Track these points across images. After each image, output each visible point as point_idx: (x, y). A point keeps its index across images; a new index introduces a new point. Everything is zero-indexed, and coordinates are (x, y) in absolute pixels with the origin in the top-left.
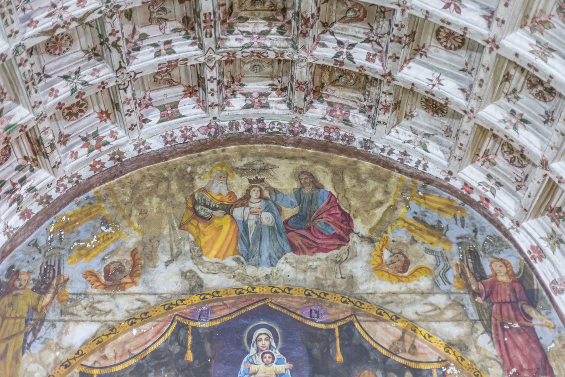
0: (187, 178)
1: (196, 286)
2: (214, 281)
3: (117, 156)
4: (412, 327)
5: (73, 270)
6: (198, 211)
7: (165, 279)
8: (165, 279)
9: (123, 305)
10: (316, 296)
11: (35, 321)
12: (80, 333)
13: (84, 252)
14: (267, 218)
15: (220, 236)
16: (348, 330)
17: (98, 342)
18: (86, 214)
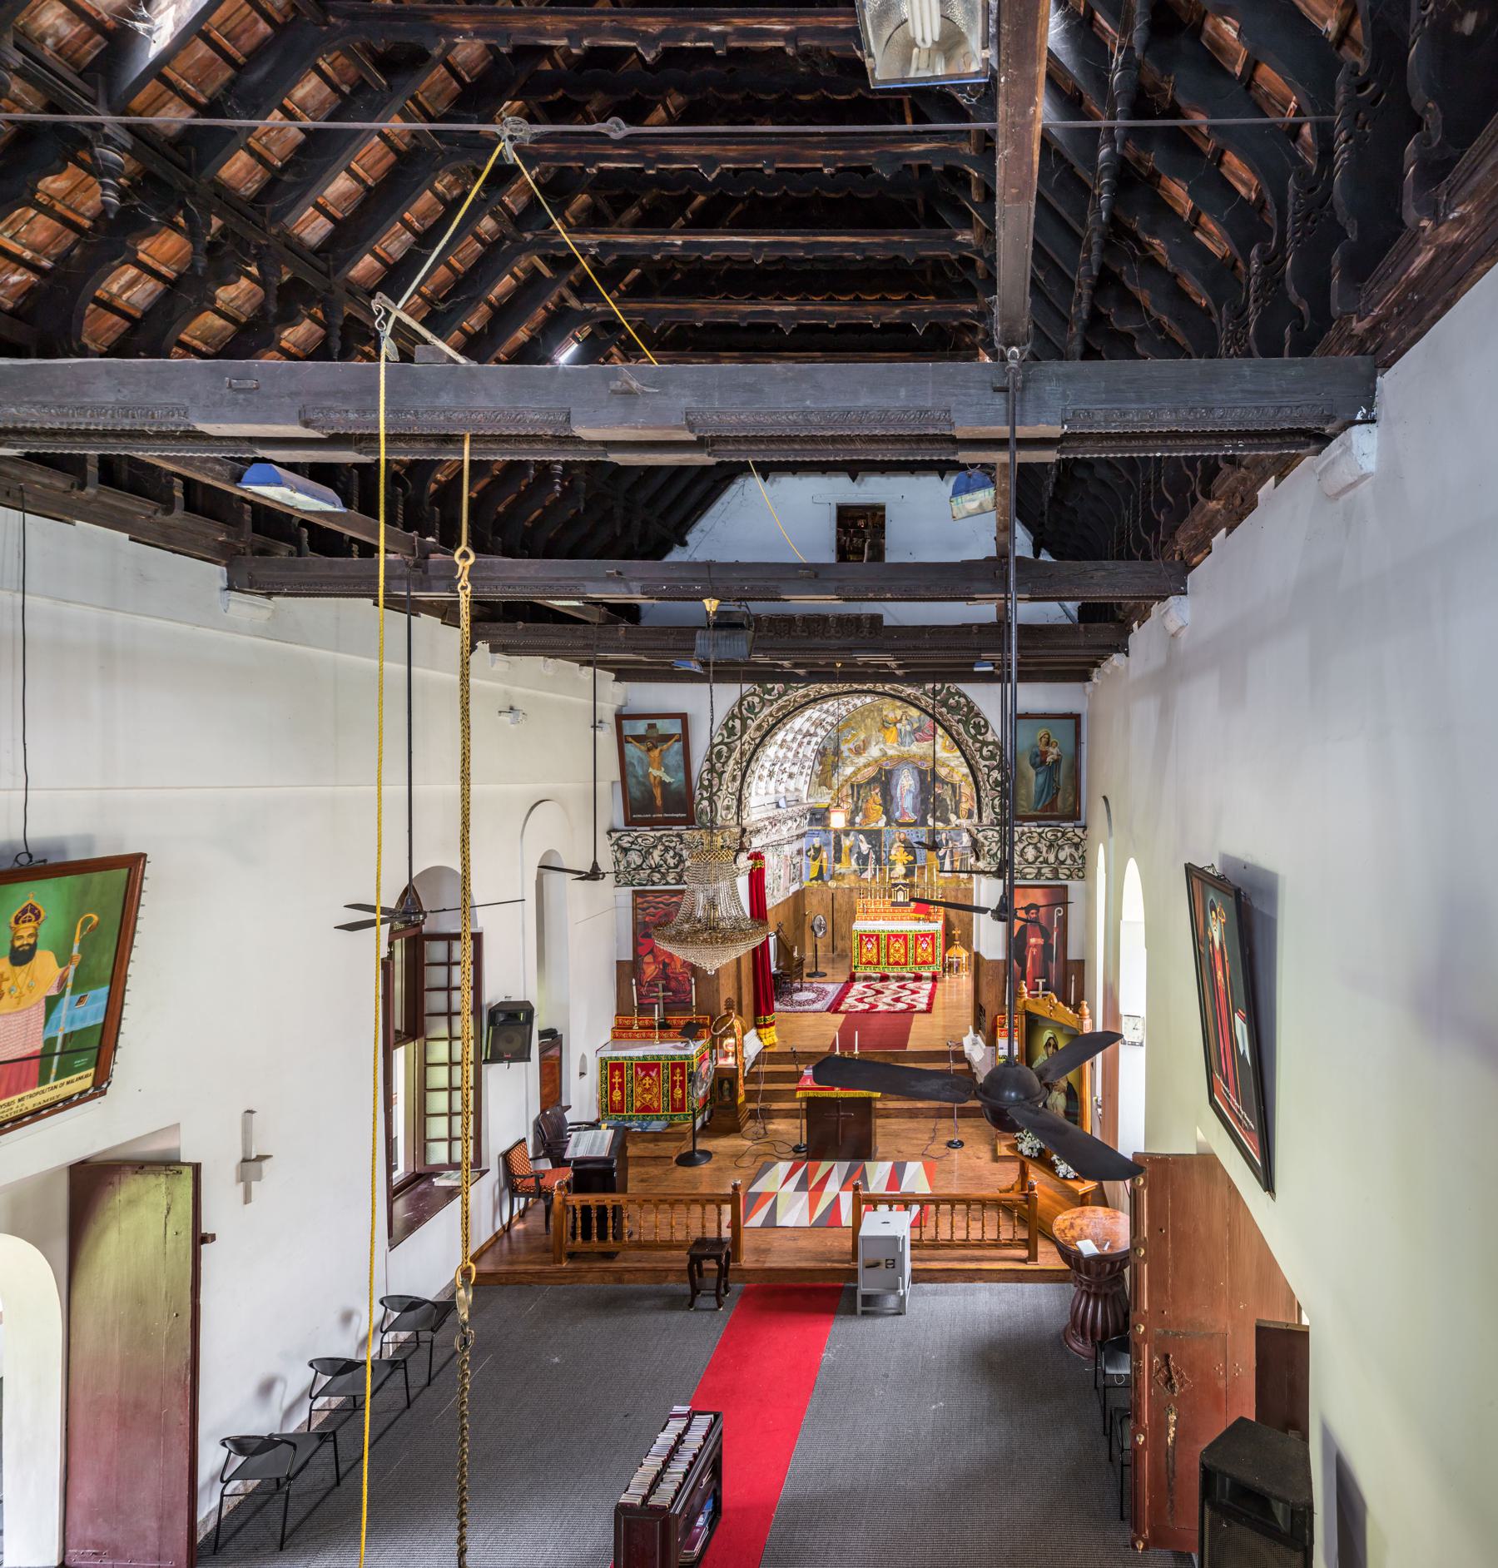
0: (881, 710)
1: (885, 754)
2: (891, 752)
3: (855, 706)
4: (952, 770)
5: (844, 747)
6: (885, 725)
7: (874, 752)
8: (874, 752)
9: (861, 761)
10: (923, 758)
11: (835, 767)
12: (849, 770)
13: (847, 741)
14: (908, 728)
15: (892, 734)
16: (933, 770)
17: (854, 773)
18: (847, 725)
